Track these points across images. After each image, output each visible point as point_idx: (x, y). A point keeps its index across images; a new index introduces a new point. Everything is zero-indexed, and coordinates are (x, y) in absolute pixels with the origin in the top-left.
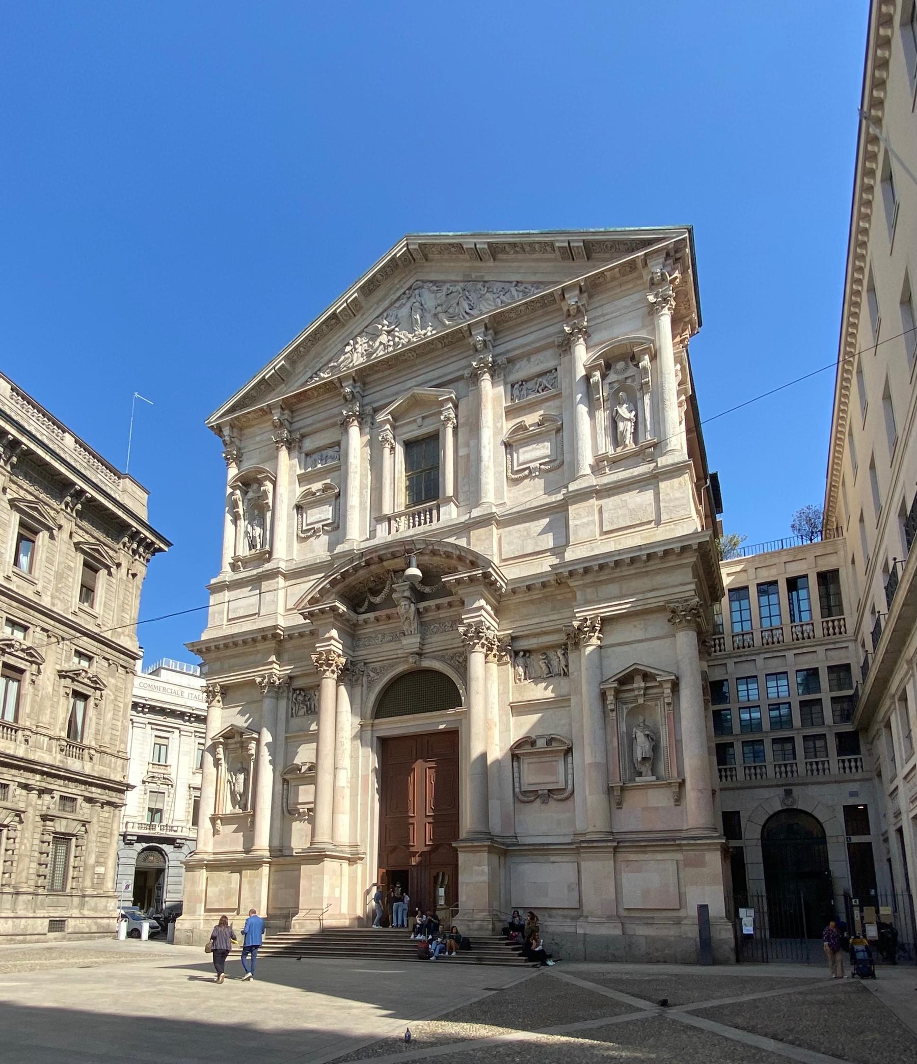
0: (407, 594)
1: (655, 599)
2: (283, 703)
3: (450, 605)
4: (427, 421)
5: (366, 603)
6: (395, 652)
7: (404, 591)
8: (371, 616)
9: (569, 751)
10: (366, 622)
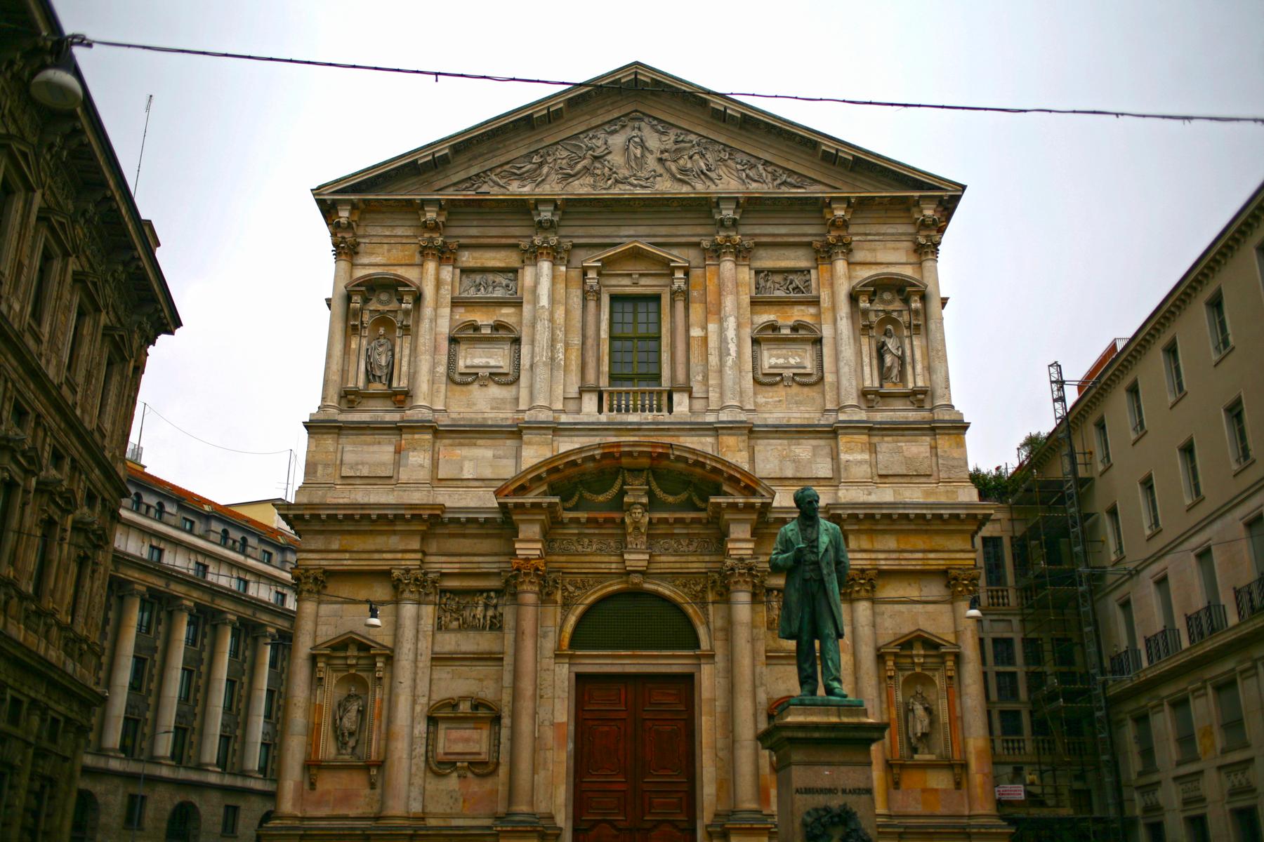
0: (645, 500)
1: (936, 561)
2: (428, 611)
3: (694, 521)
4: (643, 281)
5: (576, 498)
6: (608, 566)
7: (641, 496)
8: (583, 516)
10: (576, 521)
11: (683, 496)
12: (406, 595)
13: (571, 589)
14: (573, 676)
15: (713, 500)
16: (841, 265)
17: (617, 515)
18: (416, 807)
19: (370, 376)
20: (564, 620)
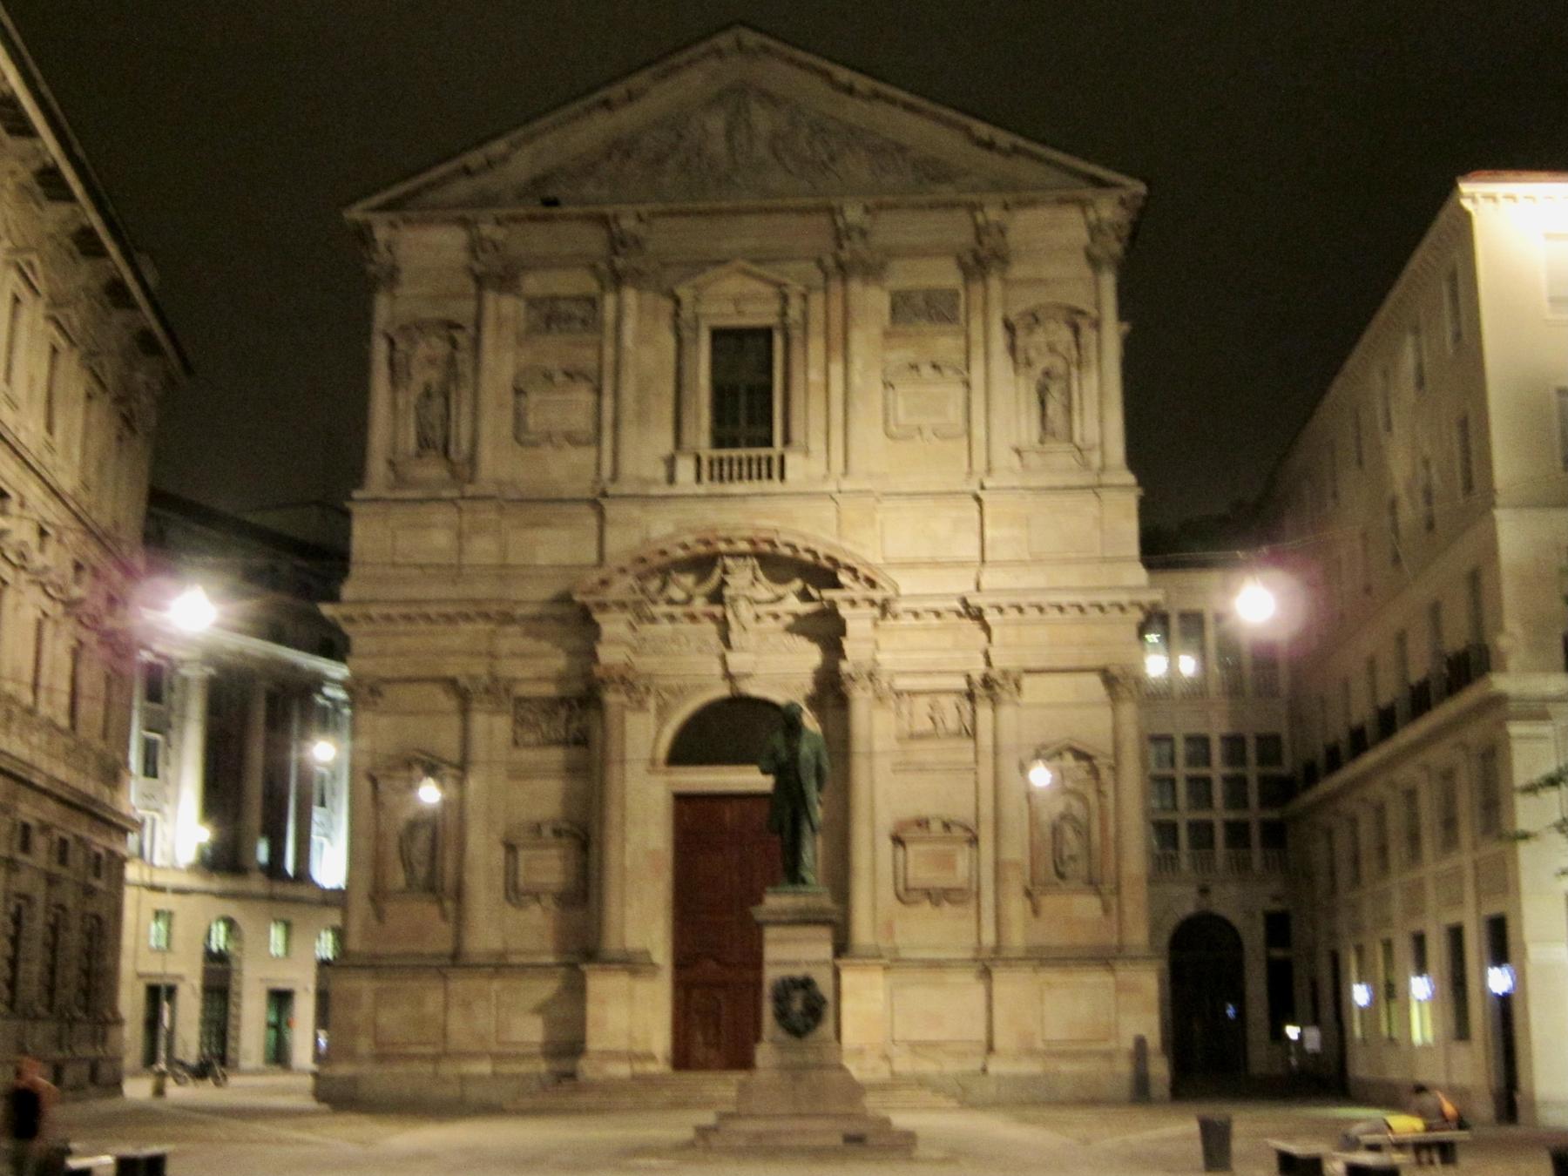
9: (974, 841)
11: (797, 584)
12: (475, 705)
13: (666, 696)
14: (670, 797)
15: (829, 594)
16: (995, 284)
17: (717, 610)
18: (496, 944)
19: (424, 443)
20: (659, 733)
